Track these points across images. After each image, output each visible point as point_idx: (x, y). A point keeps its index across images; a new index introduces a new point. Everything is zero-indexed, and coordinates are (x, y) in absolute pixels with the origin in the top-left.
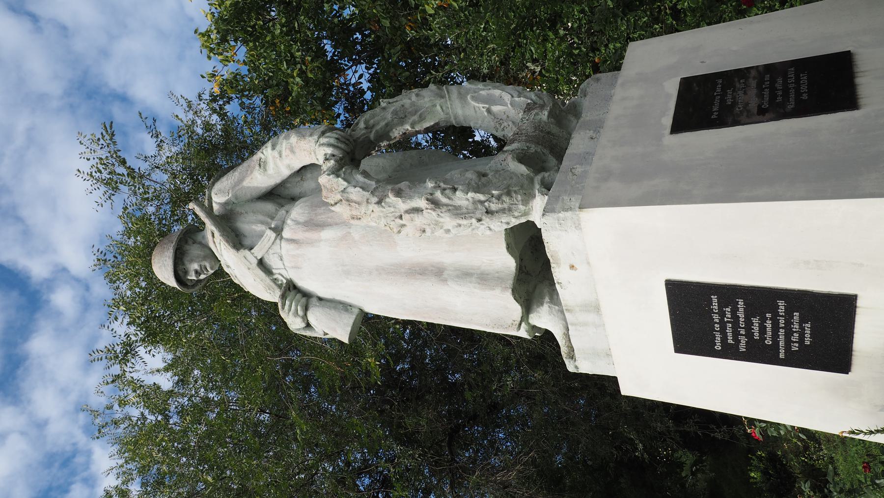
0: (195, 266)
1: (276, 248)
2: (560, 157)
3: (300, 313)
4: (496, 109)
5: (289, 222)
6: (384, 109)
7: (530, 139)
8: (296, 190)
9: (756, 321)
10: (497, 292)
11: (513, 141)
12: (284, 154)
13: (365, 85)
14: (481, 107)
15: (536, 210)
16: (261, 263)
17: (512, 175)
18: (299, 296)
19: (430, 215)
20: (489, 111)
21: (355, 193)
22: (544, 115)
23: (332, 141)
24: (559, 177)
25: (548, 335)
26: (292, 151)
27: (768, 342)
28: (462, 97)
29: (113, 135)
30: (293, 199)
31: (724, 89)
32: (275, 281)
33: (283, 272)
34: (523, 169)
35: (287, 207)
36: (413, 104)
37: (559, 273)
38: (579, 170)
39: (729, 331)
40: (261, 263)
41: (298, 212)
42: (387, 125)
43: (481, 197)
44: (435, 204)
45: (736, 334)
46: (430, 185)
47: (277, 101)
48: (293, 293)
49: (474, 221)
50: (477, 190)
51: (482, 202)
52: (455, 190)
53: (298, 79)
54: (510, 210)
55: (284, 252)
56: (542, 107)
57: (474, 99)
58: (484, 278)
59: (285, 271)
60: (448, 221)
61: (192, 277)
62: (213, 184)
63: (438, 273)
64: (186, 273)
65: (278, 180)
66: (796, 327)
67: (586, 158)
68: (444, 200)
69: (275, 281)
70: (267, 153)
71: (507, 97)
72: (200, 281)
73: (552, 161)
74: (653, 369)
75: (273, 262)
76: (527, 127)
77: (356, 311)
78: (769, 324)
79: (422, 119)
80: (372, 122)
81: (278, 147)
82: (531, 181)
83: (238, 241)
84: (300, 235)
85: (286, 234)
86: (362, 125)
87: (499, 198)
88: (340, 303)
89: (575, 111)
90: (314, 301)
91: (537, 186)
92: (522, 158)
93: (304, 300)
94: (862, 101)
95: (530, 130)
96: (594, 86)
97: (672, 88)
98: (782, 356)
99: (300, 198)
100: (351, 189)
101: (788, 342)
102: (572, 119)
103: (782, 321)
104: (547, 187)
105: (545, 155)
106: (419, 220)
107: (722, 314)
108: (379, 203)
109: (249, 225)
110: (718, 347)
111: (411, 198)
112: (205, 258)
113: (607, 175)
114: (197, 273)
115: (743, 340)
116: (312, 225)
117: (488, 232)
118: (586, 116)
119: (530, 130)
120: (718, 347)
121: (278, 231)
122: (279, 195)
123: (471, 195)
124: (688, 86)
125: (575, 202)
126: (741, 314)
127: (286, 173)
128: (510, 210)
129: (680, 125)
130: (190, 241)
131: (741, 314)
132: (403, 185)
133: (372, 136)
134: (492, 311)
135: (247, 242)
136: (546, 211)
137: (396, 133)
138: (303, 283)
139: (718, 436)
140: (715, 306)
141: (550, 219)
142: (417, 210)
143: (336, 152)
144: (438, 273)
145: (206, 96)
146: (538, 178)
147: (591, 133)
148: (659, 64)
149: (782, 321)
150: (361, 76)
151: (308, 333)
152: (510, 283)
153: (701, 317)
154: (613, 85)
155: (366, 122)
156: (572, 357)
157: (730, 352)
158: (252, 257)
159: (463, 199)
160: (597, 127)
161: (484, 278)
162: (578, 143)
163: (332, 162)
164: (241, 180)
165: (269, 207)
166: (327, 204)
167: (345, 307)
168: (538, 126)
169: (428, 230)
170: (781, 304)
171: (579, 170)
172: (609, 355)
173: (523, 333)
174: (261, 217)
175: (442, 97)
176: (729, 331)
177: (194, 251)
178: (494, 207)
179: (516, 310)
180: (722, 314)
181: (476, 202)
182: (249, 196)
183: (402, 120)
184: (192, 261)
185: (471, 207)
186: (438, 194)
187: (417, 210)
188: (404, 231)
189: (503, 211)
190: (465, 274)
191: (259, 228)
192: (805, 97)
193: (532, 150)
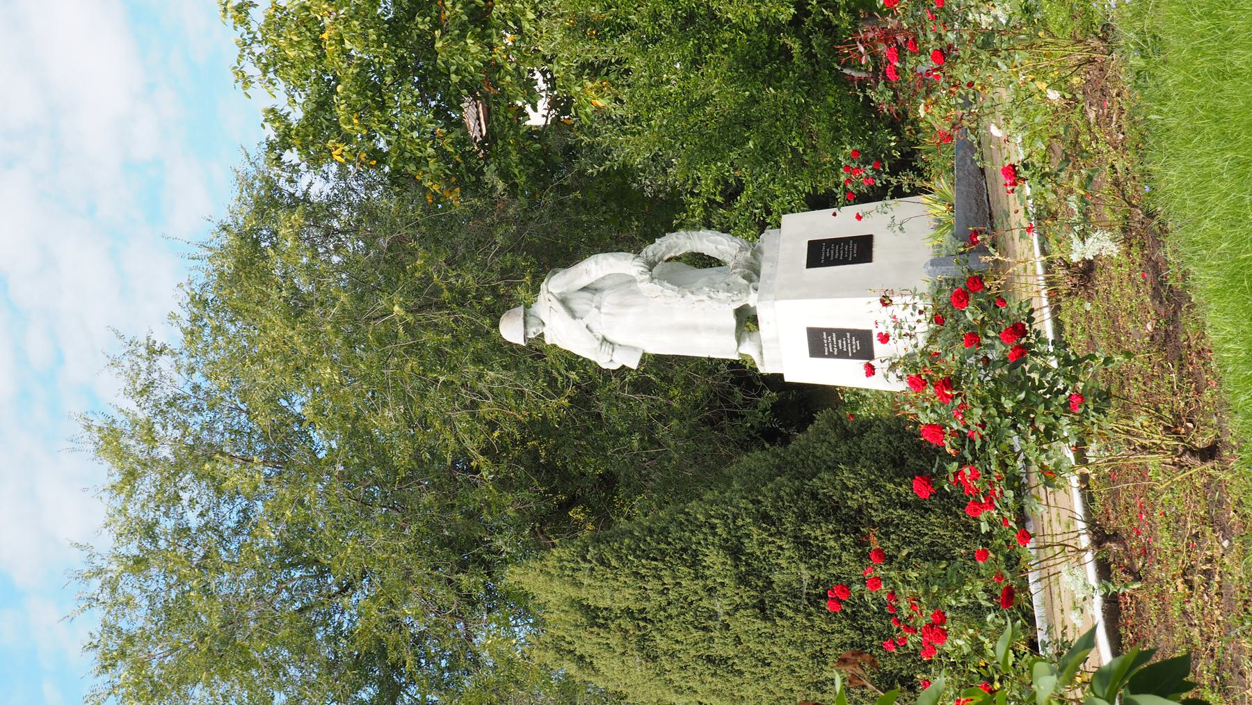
0: (534, 329)
2: (758, 276)
8: (599, 286)
14: (712, 246)
19: (709, 302)
21: (668, 292)
22: (749, 254)
28: (700, 239)
34: (745, 282)
41: (608, 299)
59: (601, 331)
63: (695, 328)
67: (771, 276)
73: (755, 277)
74: (802, 368)
75: (593, 326)
76: (741, 258)
86: (650, 254)
91: (752, 290)
96: (769, 234)
106: (702, 305)
109: (579, 303)
116: (621, 305)
118: (767, 254)
121: (598, 308)
124: (812, 244)
129: (808, 267)
138: (609, 338)
144: (695, 328)
157: (831, 355)
158: (583, 324)
159: (723, 295)
160: (774, 261)
161: (720, 330)
162: (765, 269)
165: (587, 295)
167: (636, 349)
177: (532, 320)
179: (736, 343)
190: (710, 329)
191: (587, 307)
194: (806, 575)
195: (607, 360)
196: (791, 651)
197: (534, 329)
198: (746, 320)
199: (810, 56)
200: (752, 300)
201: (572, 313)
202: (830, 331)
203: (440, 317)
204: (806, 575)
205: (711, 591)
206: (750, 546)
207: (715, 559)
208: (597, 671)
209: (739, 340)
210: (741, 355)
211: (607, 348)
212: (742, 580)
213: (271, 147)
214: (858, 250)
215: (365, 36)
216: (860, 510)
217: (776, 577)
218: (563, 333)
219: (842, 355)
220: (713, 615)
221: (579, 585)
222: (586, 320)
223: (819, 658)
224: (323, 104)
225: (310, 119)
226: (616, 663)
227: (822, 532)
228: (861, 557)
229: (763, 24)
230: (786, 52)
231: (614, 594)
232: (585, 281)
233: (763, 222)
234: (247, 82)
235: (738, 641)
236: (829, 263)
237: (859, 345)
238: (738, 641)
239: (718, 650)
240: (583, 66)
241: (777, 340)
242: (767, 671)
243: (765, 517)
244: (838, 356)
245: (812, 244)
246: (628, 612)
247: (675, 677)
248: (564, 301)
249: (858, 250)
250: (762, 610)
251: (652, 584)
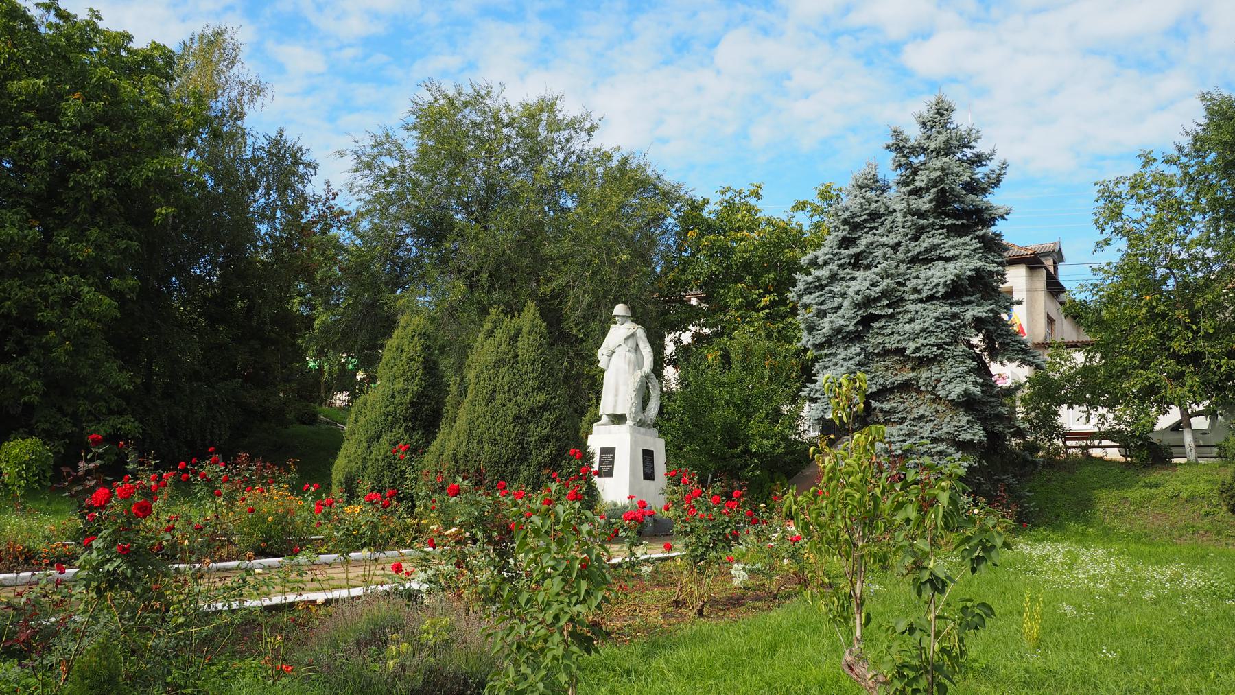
15: (629, 422)
41: (632, 356)
58: (615, 406)
63: (617, 395)
105: (641, 424)
109: (631, 342)
129: (644, 451)
134: (607, 405)
144: (617, 395)
148: (659, 446)
153: (608, 452)
160: (645, 434)
161: (615, 406)
162: (642, 430)
190: (616, 402)
194: (533, 439)
195: (602, 354)
196: (498, 430)
198: (618, 419)
199: (733, 456)
200: (629, 422)
201: (627, 339)
202: (613, 457)
203: (615, 276)
204: (533, 439)
205: (526, 395)
206: (546, 414)
207: (542, 397)
208: (487, 338)
212: (531, 410)
213: (693, 201)
214: (649, 475)
215: (746, 251)
216: (559, 466)
217: (532, 426)
220: (515, 395)
221: (530, 333)
223: (494, 442)
224: (709, 228)
225: (704, 220)
226: (492, 348)
227: (551, 448)
228: (539, 465)
229: (747, 437)
230: (735, 446)
231: (525, 348)
232: (641, 345)
233: (662, 433)
234: (723, 193)
235: (504, 405)
236: (644, 458)
238: (504, 405)
239: (499, 396)
240: (727, 351)
242: (488, 418)
243: (559, 422)
246: (516, 356)
247: (485, 375)
248: (633, 335)
249: (649, 475)
250: (517, 418)
251: (530, 368)
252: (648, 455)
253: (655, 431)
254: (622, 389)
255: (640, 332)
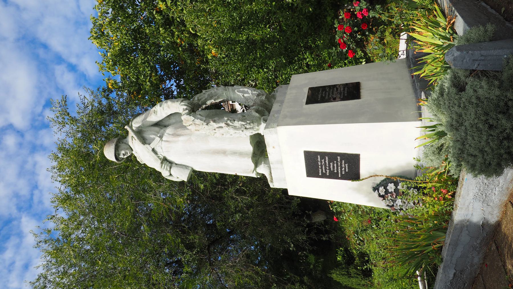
0: (123, 152)
1: (160, 144)
2: (269, 112)
3: (168, 169)
4: (246, 95)
5: (165, 134)
6: (204, 93)
7: (259, 105)
8: (167, 123)
9: (331, 164)
10: (246, 159)
11: (252, 106)
12: (165, 109)
13: (174, 88)
15: (261, 129)
16: (153, 150)
17: (254, 117)
18: (168, 163)
19: (226, 129)
20: (243, 96)
21: (198, 121)
23: (186, 104)
24: (269, 118)
25: (263, 175)
26: (169, 107)
27: (335, 171)
29: (66, 101)
30: (166, 126)
31: (322, 91)
32: (158, 157)
33: (162, 153)
34: (257, 115)
35: (164, 129)
36: (215, 92)
37: (269, 150)
38: (276, 115)
39: (323, 168)
40: (153, 150)
41: (169, 130)
42: (206, 99)
43: (244, 123)
44: (228, 125)
45: (326, 169)
46: (226, 119)
47: (135, 92)
48: (166, 162)
49: (241, 131)
50: (242, 121)
51: (244, 125)
52: (234, 120)
53: (148, 83)
54: (253, 128)
55: (163, 146)
56: (263, 95)
57: (238, 91)
58: (241, 154)
59: (162, 153)
60: (232, 131)
61: (121, 156)
62: (133, 120)
63: (224, 153)
64: (119, 155)
65: (161, 119)
66: (343, 165)
67: (279, 112)
68: (231, 124)
69: (158, 157)
70: (157, 107)
71: (250, 91)
72: (123, 159)
73: (267, 113)
75: (158, 149)
76: (258, 101)
77: (190, 169)
78: (335, 165)
79: (218, 98)
80: (200, 98)
81: (162, 106)
82: (260, 119)
83: (144, 141)
84: (171, 139)
85: (164, 139)
86: (196, 99)
87: (249, 124)
88: (184, 165)
89: (274, 97)
90: (174, 165)
92: (257, 111)
93: (170, 164)
94: (361, 97)
95: (259, 103)
97: (306, 90)
98: (340, 176)
99: (168, 126)
100: (196, 120)
101: (341, 171)
102: (273, 100)
103: (339, 164)
104: (265, 121)
105: (264, 111)
107: (321, 162)
108: (207, 124)
109: (149, 135)
110: (320, 174)
111: (219, 123)
112: (127, 149)
113: (285, 117)
114: (124, 155)
115: (328, 171)
116: (175, 135)
117: (245, 136)
118: (278, 99)
119: (259, 103)
120: (320, 174)
121: (161, 137)
122: (160, 125)
123: (240, 122)
125: (275, 125)
126: (327, 162)
127: (164, 116)
128: (253, 128)
129: (307, 103)
130: (121, 142)
131: (327, 162)
132: (216, 119)
133: (200, 103)
134: (243, 167)
135: (147, 142)
136: (266, 128)
137: (209, 103)
138: (169, 158)
139: (324, 239)
140: (319, 159)
141: (267, 130)
142: (221, 127)
143: (188, 108)
144: (224, 153)
145: (101, 90)
146: (263, 117)
147: (279, 104)
148: (302, 82)
149: (339, 164)
150: (172, 85)
151: (170, 178)
152: (251, 155)
154: (287, 89)
155: (198, 98)
156: (272, 182)
157: (324, 176)
158: (149, 148)
159: (237, 124)
160: (282, 102)
161: (241, 154)
162: (275, 107)
163: (187, 111)
164: (146, 118)
165: (156, 129)
166: (185, 127)
167: (186, 167)
168: (262, 101)
169: (225, 134)
170: (339, 157)
171: (276, 115)
172: (285, 180)
173: (254, 175)
174: (154, 133)
175: (226, 90)
176: (323, 168)
177: (122, 146)
178: (248, 126)
179: (252, 165)
180: (321, 162)
181: (241, 125)
182: (148, 125)
183: (211, 98)
184: (122, 150)
185: (240, 126)
186: (229, 122)
187: (221, 127)
188: (216, 135)
189: (250, 128)
190: (234, 153)
191: (152, 136)
192: (346, 95)
193: (260, 109)
197: (123, 152)
202: (323, 155)
209: (256, 165)
210: (258, 174)
211: (167, 166)
218: (143, 154)
219: (333, 176)
222: (153, 145)
236: (323, 100)
237: (347, 167)
241: (281, 162)
244: (330, 177)
245: (310, 89)
248: (140, 133)
252: (317, 95)
253: (280, 90)
254: (213, 144)
255: (136, 123)
